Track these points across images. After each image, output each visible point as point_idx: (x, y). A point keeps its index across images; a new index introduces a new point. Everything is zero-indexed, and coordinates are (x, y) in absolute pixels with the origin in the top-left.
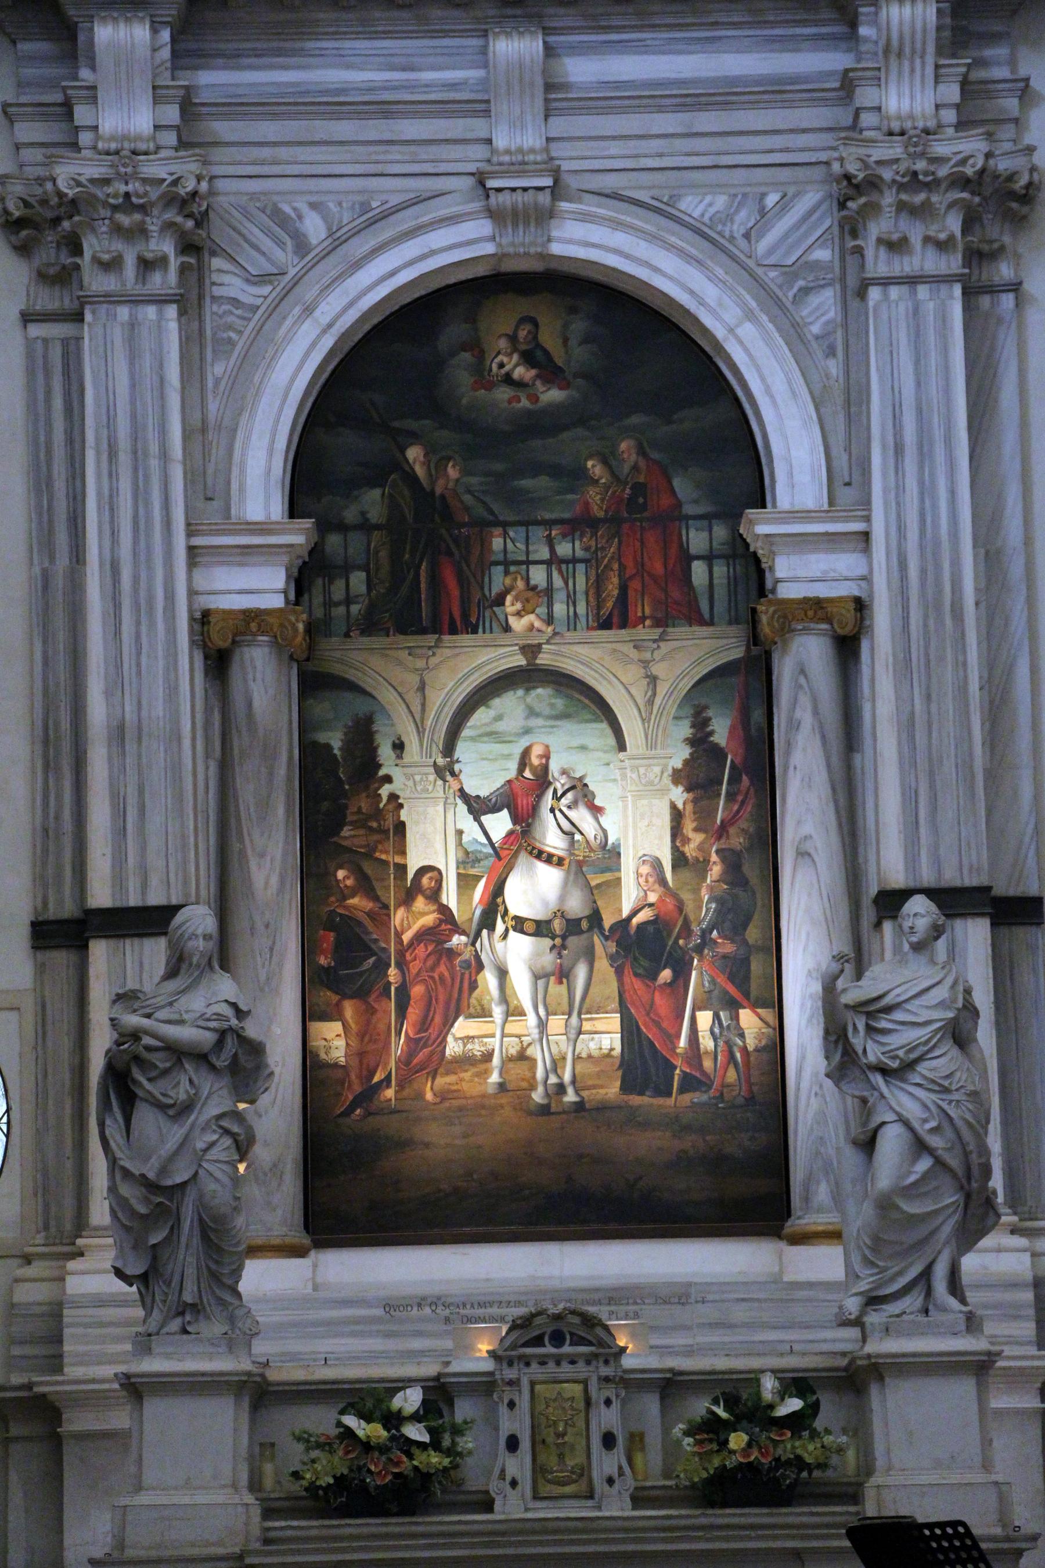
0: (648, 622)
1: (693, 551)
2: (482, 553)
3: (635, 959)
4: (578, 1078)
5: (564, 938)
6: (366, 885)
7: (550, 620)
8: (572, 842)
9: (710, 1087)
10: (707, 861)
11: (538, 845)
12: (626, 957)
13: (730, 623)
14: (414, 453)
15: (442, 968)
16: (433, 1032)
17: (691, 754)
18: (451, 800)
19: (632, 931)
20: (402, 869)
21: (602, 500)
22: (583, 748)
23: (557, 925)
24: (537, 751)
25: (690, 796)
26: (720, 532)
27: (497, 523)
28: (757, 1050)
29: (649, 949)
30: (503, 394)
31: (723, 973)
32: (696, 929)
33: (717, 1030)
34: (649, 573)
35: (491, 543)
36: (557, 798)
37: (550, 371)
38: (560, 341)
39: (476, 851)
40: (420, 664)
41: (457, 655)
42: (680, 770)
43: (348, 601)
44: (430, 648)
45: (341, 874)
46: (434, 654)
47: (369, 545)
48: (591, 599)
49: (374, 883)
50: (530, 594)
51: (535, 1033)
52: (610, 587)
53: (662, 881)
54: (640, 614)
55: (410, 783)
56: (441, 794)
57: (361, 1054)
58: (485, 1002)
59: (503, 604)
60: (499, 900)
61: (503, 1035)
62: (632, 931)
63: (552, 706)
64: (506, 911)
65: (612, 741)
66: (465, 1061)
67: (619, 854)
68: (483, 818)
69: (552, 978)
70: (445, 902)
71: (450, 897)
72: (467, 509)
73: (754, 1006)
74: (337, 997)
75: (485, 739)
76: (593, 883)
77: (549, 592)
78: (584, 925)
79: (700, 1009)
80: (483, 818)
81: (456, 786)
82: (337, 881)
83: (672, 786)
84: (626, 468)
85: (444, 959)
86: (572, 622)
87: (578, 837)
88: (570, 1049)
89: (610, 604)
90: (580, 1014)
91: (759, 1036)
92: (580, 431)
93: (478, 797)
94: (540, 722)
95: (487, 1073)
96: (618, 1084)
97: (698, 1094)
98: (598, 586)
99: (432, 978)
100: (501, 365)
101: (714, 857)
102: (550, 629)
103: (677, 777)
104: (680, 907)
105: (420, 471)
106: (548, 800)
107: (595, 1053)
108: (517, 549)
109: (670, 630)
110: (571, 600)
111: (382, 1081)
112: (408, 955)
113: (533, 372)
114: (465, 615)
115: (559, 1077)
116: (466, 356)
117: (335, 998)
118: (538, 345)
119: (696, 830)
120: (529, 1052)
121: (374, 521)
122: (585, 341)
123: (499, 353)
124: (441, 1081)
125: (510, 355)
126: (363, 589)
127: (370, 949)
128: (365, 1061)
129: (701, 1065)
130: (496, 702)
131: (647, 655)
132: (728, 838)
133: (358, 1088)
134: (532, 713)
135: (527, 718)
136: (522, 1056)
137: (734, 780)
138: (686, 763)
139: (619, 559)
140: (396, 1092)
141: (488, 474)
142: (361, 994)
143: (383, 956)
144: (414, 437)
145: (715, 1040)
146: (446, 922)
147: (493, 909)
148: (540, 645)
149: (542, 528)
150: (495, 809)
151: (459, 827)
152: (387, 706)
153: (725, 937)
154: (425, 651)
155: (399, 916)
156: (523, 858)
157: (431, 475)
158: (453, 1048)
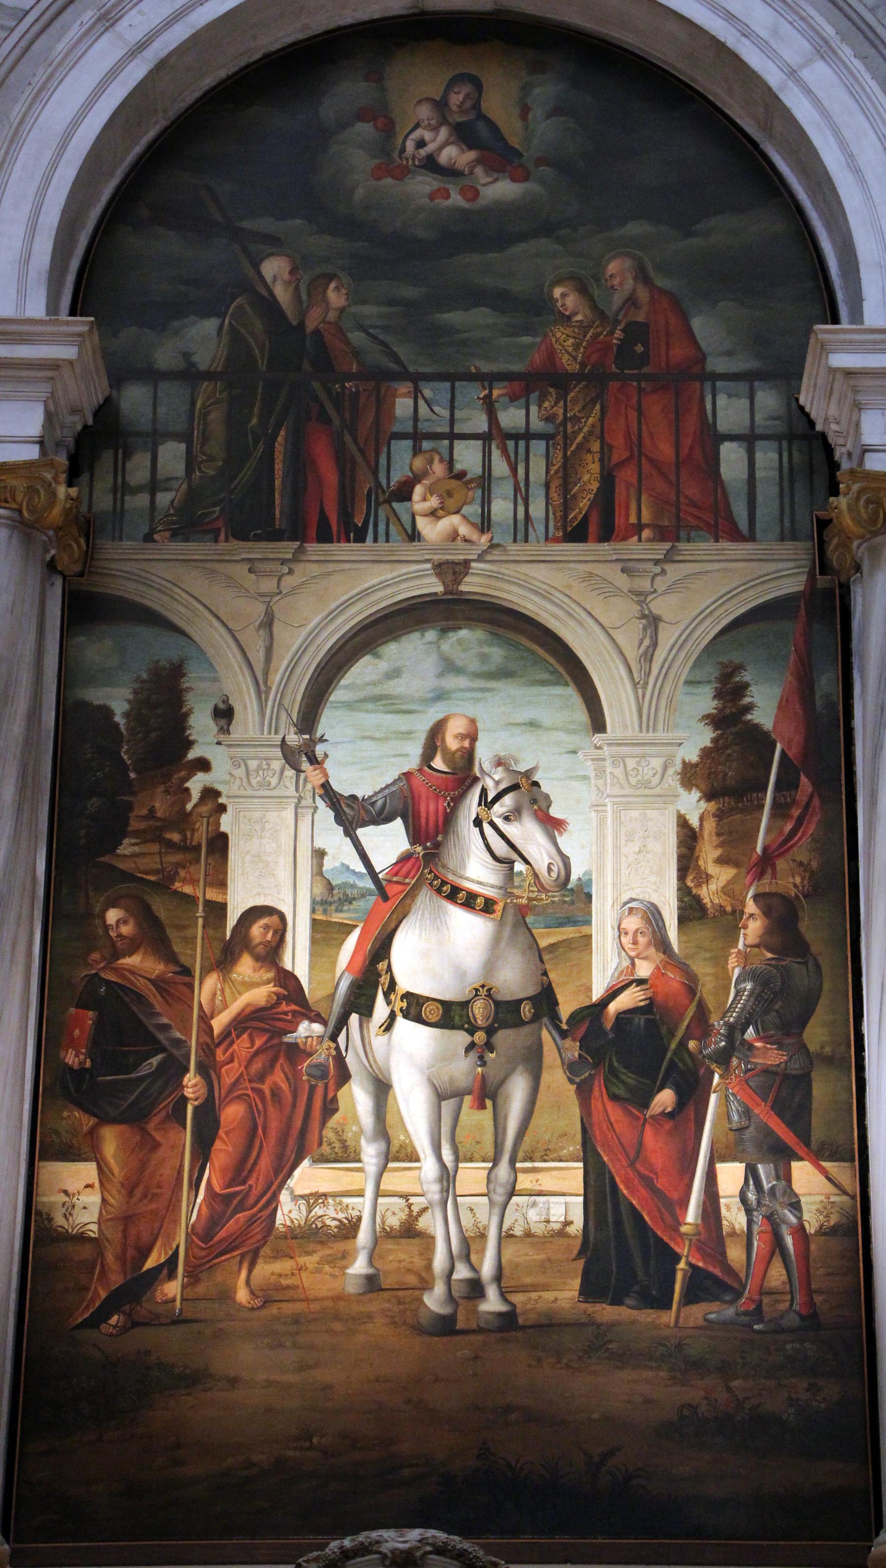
0: (646, 533)
1: (723, 426)
2: (377, 423)
3: (613, 1071)
4: (506, 1271)
5: (490, 1031)
6: (154, 936)
7: (485, 524)
8: (510, 874)
9: (739, 1294)
10: (738, 913)
11: (451, 877)
12: (596, 1066)
13: (782, 538)
14: (274, 268)
15: (278, 1077)
16: (256, 1183)
17: (715, 741)
18: (307, 801)
19: (608, 1025)
20: (218, 910)
21: (577, 346)
22: (533, 725)
23: (479, 1011)
24: (456, 727)
25: (712, 806)
26: (768, 400)
27: (404, 375)
28: (822, 1232)
29: (636, 1055)
30: (422, 185)
31: (765, 1100)
32: (717, 1023)
33: (752, 1196)
34: (650, 460)
35: (394, 403)
36: (486, 803)
37: (499, 156)
38: (516, 111)
39: (346, 885)
40: (268, 585)
41: (329, 574)
42: (696, 765)
43: (154, 486)
44: (284, 562)
45: (113, 916)
46: (291, 572)
47: (193, 403)
48: (554, 494)
49: (169, 931)
50: (454, 483)
51: (434, 1191)
52: (586, 478)
53: (663, 944)
54: (633, 519)
55: (240, 772)
56: (292, 791)
57: (127, 1220)
58: (349, 1136)
59: (409, 498)
60: (382, 966)
61: (378, 1193)
62: (608, 1025)
63: (484, 658)
64: (393, 984)
65: (581, 716)
66: (310, 1235)
67: (589, 896)
68: (360, 832)
69: (468, 1099)
70: (288, 966)
71: (298, 958)
72: (356, 353)
73: (819, 1154)
74: (93, 1121)
75: (370, 706)
76: (543, 943)
77: (485, 481)
78: (526, 1011)
79: (724, 1159)
80: (360, 832)
81: (315, 777)
82: (106, 927)
83: (681, 791)
84: (617, 300)
85: (281, 1061)
86: (521, 530)
87: (519, 867)
88: (495, 1220)
89: (584, 504)
90: (513, 1161)
91: (825, 1209)
92: (544, 244)
93: (354, 797)
94: (462, 682)
95: (347, 1257)
96: (577, 1283)
97: (715, 1306)
98: (564, 477)
99: (259, 1092)
100: (421, 144)
101: (751, 907)
102: (484, 539)
103: (689, 775)
104: (691, 989)
105: (282, 294)
106: (471, 806)
107: (538, 1229)
108: (435, 416)
109: (681, 546)
110: (522, 494)
111: (158, 1268)
112: (219, 1052)
113: (472, 155)
114: (346, 515)
115: (473, 1268)
116: (365, 129)
117: (88, 1122)
118: (481, 116)
119: (721, 861)
120: (422, 1224)
121: (203, 367)
122: (556, 111)
123: (417, 126)
124: (265, 1270)
125: (435, 129)
126: (179, 469)
127: (157, 1041)
128: (133, 1231)
129: (724, 1254)
130: (391, 650)
131: (645, 584)
132: (774, 876)
133: (116, 1279)
134: (449, 667)
135: (441, 675)
136: (409, 1231)
137: (787, 783)
138: (706, 753)
139: (602, 439)
140: (184, 1287)
141: (392, 303)
142: (135, 1117)
143: (175, 1052)
144: (275, 244)
145: (749, 1211)
146: (288, 999)
147: (370, 979)
148: (466, 563)
149: (477, 384)
150: (382, 818)
151: (319, 844)
152: (210, 652)
153: (766, 1039)
154: (277, 566)
155: (207, 988)
156: (425, 898)
157: (299, 300)
158: (288, 1212)
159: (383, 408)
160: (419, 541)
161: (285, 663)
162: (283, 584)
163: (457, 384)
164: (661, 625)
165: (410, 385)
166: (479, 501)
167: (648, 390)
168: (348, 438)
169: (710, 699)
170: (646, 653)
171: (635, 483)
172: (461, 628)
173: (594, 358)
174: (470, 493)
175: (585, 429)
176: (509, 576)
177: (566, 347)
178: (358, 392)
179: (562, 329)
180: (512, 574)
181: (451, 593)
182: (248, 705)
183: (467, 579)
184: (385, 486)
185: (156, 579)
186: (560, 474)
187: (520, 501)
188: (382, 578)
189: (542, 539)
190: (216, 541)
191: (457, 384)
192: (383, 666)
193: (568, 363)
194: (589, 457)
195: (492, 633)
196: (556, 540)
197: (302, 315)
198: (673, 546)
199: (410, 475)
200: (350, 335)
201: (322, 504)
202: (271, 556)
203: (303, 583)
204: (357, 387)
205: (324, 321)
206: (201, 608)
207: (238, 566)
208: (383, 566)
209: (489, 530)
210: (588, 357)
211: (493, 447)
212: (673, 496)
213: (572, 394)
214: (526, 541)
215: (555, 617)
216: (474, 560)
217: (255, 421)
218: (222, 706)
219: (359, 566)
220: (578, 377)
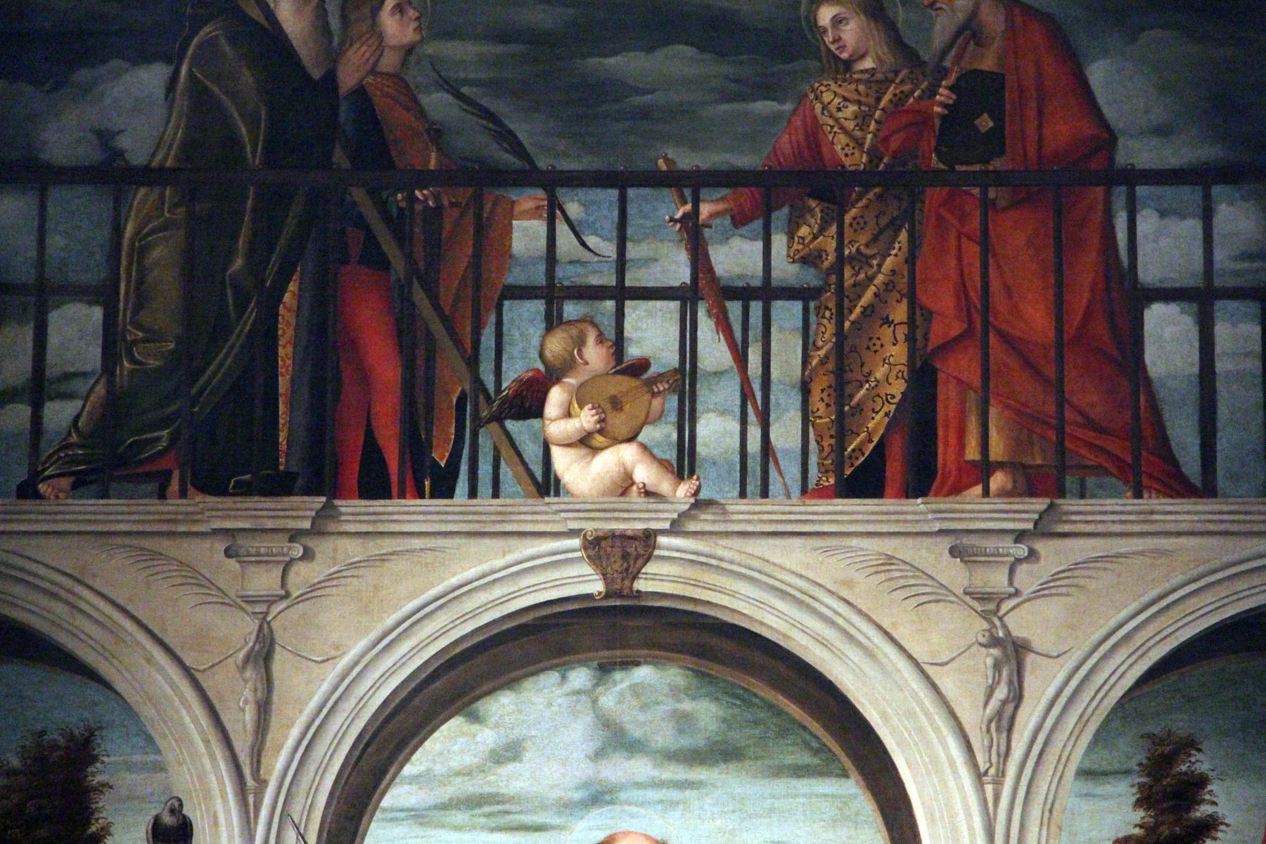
0: (998, 480)
1: (1150, 271)
7: (684, 461)
21: (863, 120)
27: (528, 176)
34: (1005, 338)
35: (508, 230)
40: (264, 581)
41: (383, 558)
44: (294, 535)
46: (308, 555)
47: (118, 230)
50: (626, 383)
52: (880, 373)
54: (972, 453)
59: (538, 412)
63: (683, 721)
72: (436, 134)
75: (460, 817)
77: (685, 380)
84: (943, 27)
86: (755, 473)
89: (877, 423)
94: (641, 768)
98: (838, 372)
102: (684, 490)
108: (588, 252)
109: (1070, 504)
110: (755, 404)
114: (415, 446)
121: (138, 157)
126: (92, 356)
130: (501, 705)
131: (997, 579)
134: (616, 739)
135: (599, 755)
141: (502, 37)
148: (648, 538)
149: (668, 194)
152: (147, 712)
159: (489, 237)
160: (557, 494)
161: (295, 732)
162: (292, 578)
163: (631, 192)
164: (1030, 659)
165: (540, 193)
166: (673, 418)
167: (1002, 203)
168: (419, 297)
169: (1130, 809)
170: (999, 714)
171: (977, 382)
172: (638, 664)
173: (894, 144)
174: (656, 403)
175: (880, 279)
176: (731, 562)
177: (843, 122)
178: (439, 209)
179: (834, 87)
180: (737, 557)
181: (619, 595)
182: (221, 816)
183: (651, 568)
184: (491, 387)
185: (42, 571)
186: (831, 366)
187: (752, 417)
188: (485, 567)
189: (796, 490)
190: (162, 495)
191: (631, 192)
192: (487, 737)
193: (845, 151)
194: (887, 332)
195: (699, 674)
196: (823, 493)
197: (333, 58)
198: (1051, 506)
199: (542, 368)
200: (425, 100)
201: (369, 425)
202: (270, 524)
203: (330, 578)
204: (437, 198)
205: (373, 71)
206: (128, 624)
207: (206, 544)
208: (487, 542)
209: (692, 473)
210: (886, 139)
211: (702, 314)
212: (1051, 408)
213: (853, 212)
214: (765, 494)
215: (823, 643)
216: (663, 532)
217: (239, 263)
218: (168, 819)
219: (441, 542)
220: (864, 179)
